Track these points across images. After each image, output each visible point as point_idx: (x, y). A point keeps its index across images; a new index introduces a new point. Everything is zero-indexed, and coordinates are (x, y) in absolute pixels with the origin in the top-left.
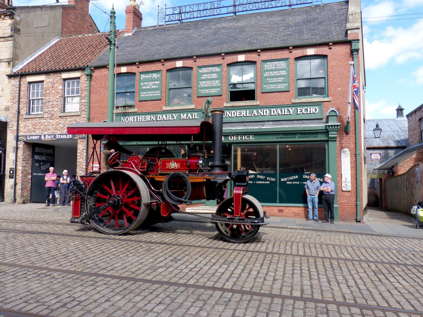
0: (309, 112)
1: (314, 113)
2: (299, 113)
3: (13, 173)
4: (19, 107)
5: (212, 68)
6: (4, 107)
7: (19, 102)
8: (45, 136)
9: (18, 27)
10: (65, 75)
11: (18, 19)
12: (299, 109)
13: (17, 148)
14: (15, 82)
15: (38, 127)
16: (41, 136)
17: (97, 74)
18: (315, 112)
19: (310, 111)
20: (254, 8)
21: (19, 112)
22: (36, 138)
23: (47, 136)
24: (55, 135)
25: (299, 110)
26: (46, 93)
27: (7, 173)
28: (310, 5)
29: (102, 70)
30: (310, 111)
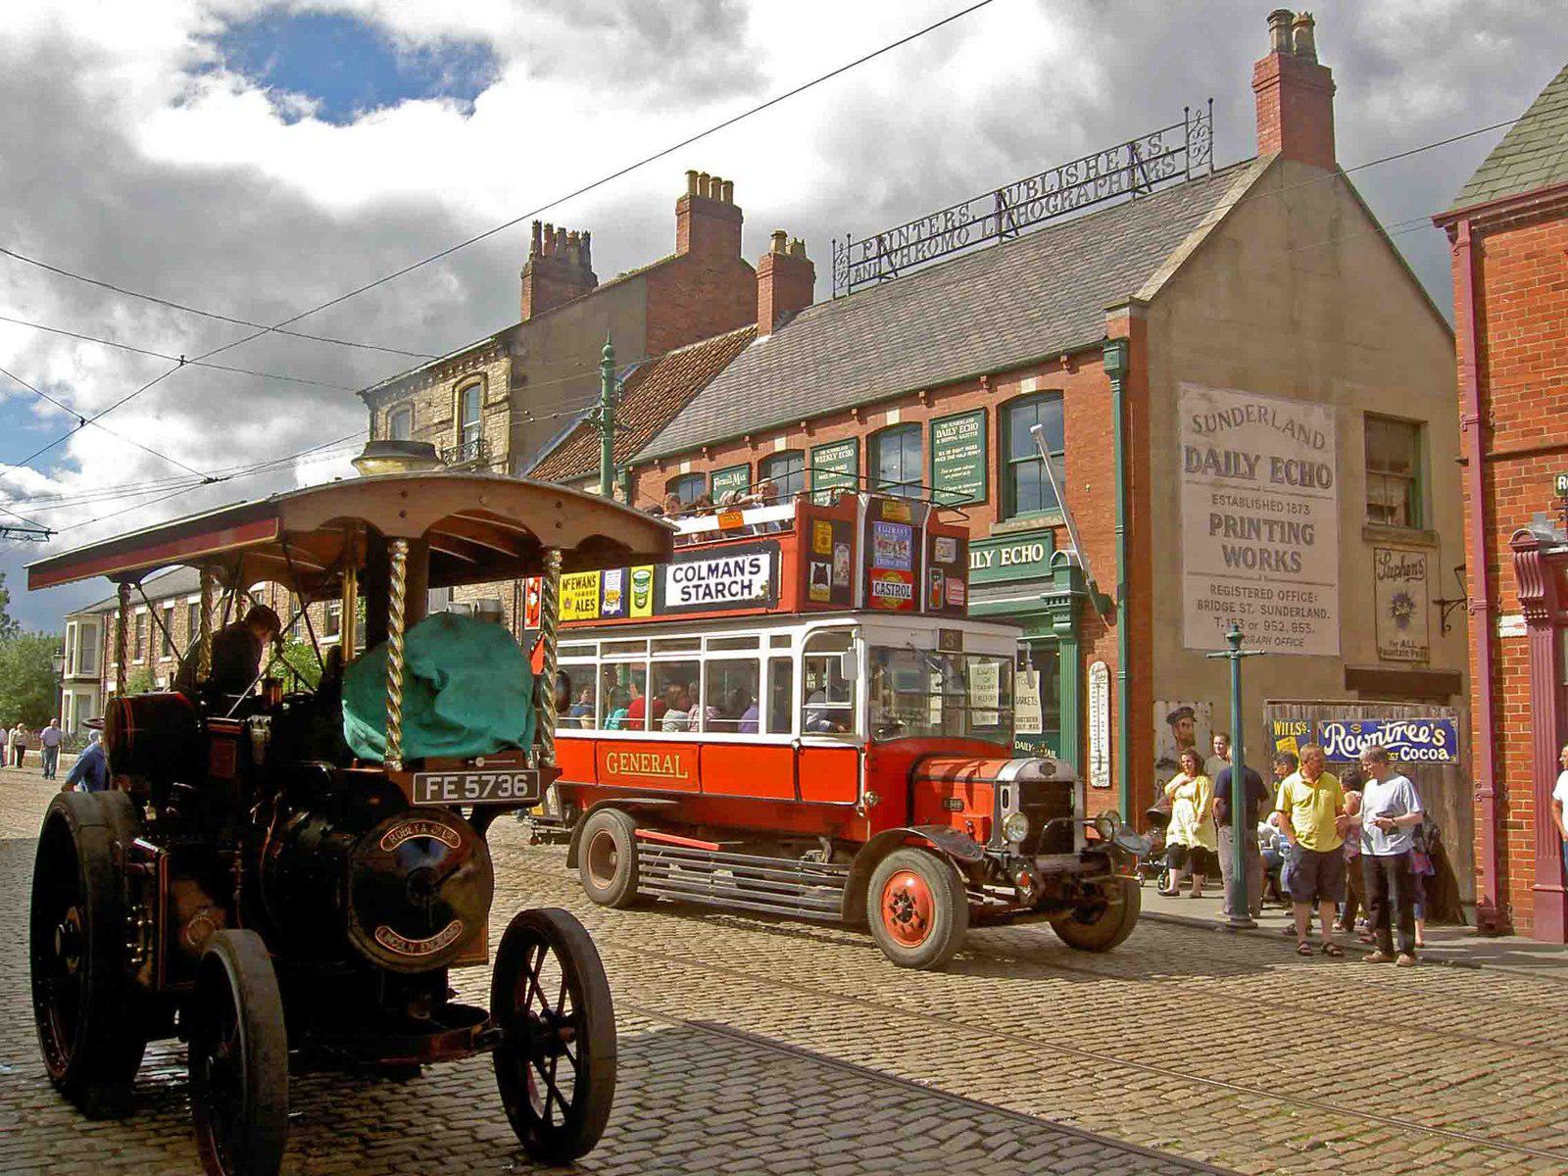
0: (1024, 560)
1: (1034, 561)
2: (1004, 562)
5: (838, 449)
9: (522, 370)
11: (521, 352)
12: (1004, 551)
18: (1036, 559)
19: (1027, 556)
20: (1046, 214)
25: (1004, 556)
28: (1182, 178)
30: (1027, 556)
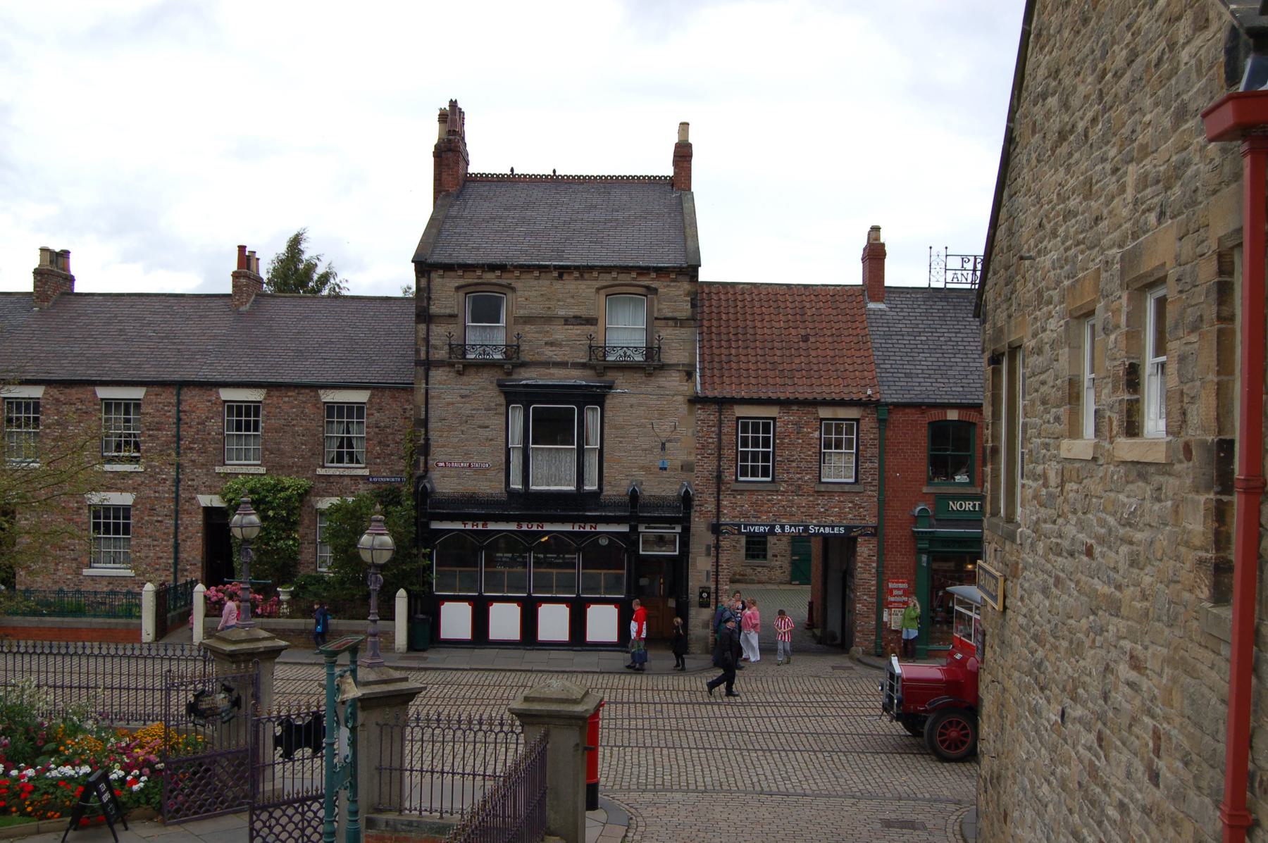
3: (709, 596)
4: (719, 466)
6: (679, 463)
7: (720, 455)
8: (782, 527)
10: (824, 413)
13: (717, 547)
14: (709, 414)
15: (765, 508)
16: (773, 527)
17: (898, 417)
21: (719, 478)
22: (762, 529)
23: (787, 528)
24: (806, 528)
26: (782, 443)
27: (693, 596)
29: (907, 410)
